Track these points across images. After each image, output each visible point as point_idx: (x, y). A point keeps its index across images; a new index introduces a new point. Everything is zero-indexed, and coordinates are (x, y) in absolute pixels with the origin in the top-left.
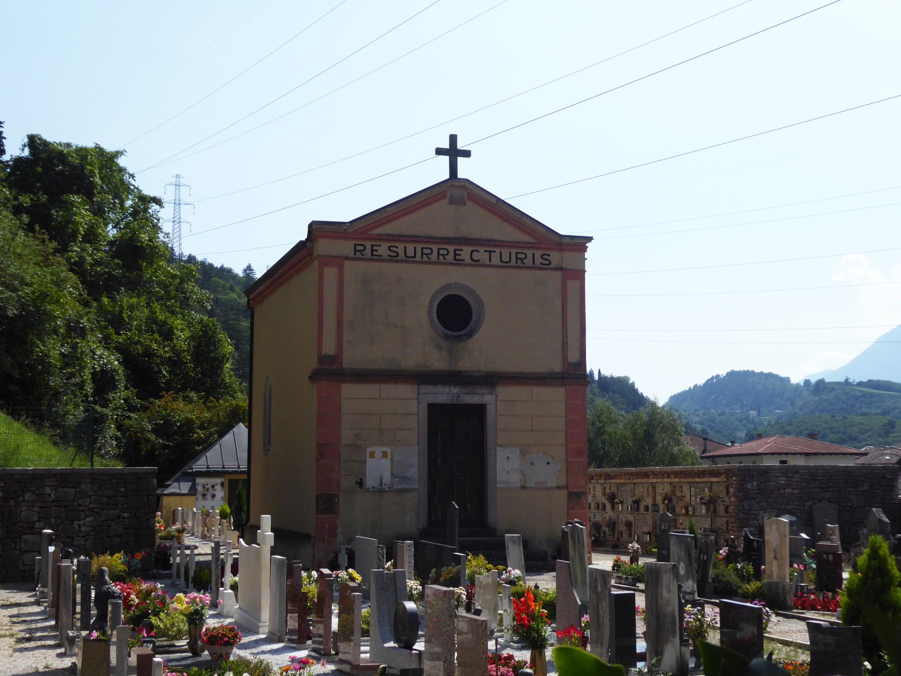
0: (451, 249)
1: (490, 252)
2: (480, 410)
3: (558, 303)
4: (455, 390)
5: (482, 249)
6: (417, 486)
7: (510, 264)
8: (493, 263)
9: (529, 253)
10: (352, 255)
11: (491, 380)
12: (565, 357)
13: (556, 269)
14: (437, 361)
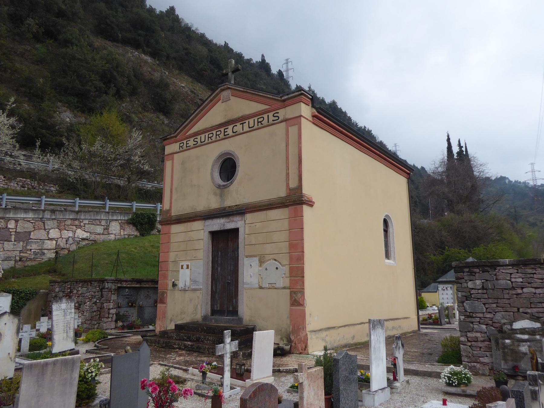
0: (222, 130)
1: (243, 124)
2: (236, 231)
3: (284, 144)
4: (222, 221)
5: (238, 124)
6: (201, 287)
7: (254, 128)
8: (245, 130)
9: (265, 116)
10: (179, 150)
11: (240, 211)
12: (288, 185)
13: (281, 122)
14: (214, 204)
